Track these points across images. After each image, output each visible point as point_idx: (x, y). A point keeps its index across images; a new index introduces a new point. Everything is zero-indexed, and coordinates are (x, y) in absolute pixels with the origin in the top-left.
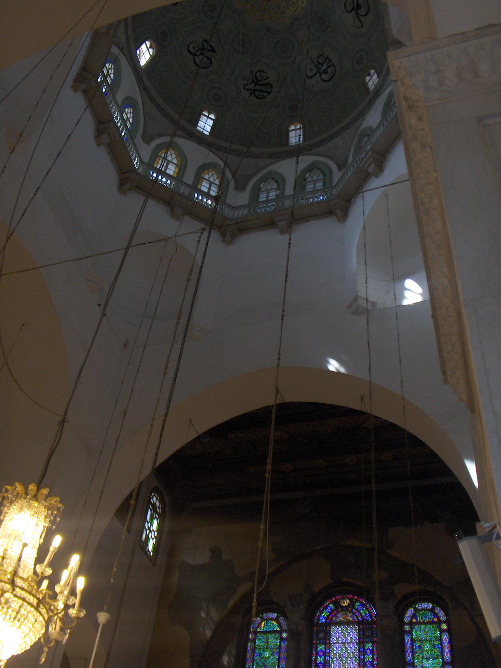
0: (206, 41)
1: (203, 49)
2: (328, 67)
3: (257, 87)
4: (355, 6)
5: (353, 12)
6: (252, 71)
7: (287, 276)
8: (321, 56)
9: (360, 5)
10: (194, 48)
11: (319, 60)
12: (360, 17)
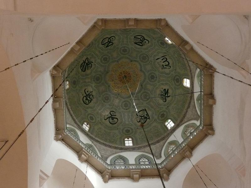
1: (110, 42)
3: (85, 64)
4: (114, 117)
6: (92, 62)
8: (93, 96)
9: (113, 120)
10: (112, 39)
11: (91, 96)
12: (109, 119)
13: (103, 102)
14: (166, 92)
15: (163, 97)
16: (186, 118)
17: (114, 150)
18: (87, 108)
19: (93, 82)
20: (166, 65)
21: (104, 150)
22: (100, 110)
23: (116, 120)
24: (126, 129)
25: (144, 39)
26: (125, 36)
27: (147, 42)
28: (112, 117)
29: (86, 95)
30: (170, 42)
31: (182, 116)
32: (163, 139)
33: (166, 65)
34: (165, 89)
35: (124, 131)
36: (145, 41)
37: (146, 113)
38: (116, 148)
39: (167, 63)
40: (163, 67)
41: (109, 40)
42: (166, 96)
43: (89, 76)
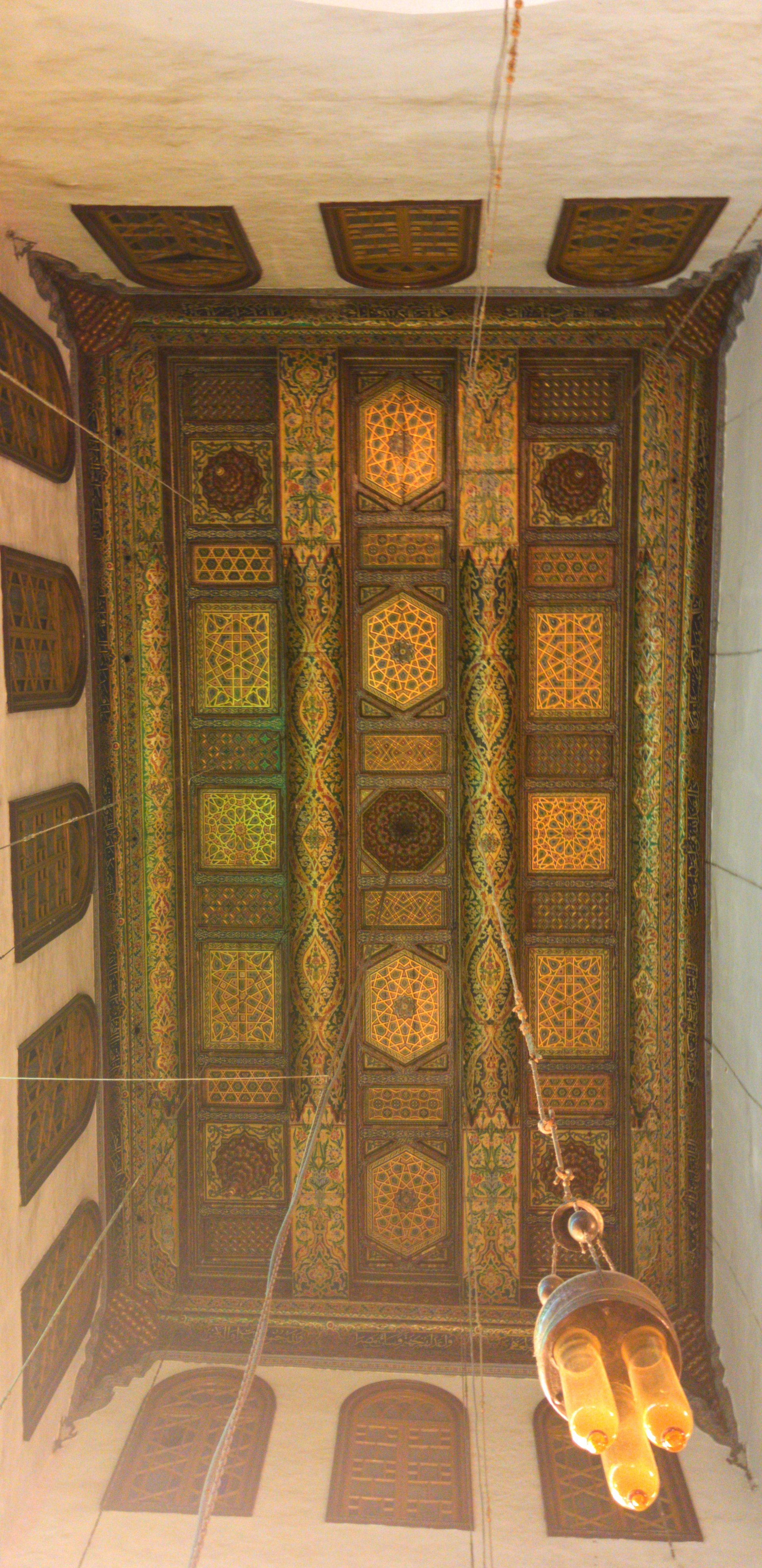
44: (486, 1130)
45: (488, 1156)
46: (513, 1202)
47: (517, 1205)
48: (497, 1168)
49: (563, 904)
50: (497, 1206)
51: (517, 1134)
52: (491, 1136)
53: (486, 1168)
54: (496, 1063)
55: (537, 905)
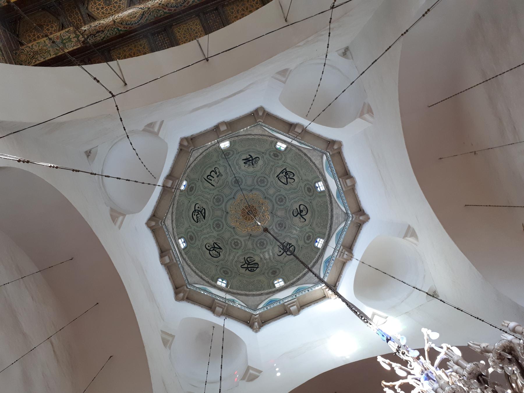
0: (216, 243)
1: (215, 247)
2: (290, 248)
3: (249, 266)
5: (299, 215)
7: (388, 49)
13: (285, 230)
14: (247, 161)
15: (255, 162)
16: (263, 133)
17: (334, 204)
18: (299, 246)
19: (267, 249)
20: (216, 174)
21: (337, 218)
22: (296, 230)
23: (302, 207)
24: (308, 193)
25: (195, 210)
26: (199, 234)
27: (197, 206)
28: (300, 213)
29: (285, 253)
30: (185, 183)
31: (265, 138)
32: (299, 150)
33: (216, 174)
34: (244, 163)
35: (311, 194)
36: (197, 208)
37: (281, 175)
38: (331, 202)
39: (213, 173)
40: (220, 175)
41: (212, 249)
42: (251, 159)
43: (261, 256)
44: (76, 35)
45: (68, 39)
46: (55, 54)
47: (54, 56)
48: (64, 44)
49: (166, 43)
50: (51, 49)
51: (79, 46)
52: (75, 37)
53: (63, 40)
54: (101, 29)
55: (162, 34)
